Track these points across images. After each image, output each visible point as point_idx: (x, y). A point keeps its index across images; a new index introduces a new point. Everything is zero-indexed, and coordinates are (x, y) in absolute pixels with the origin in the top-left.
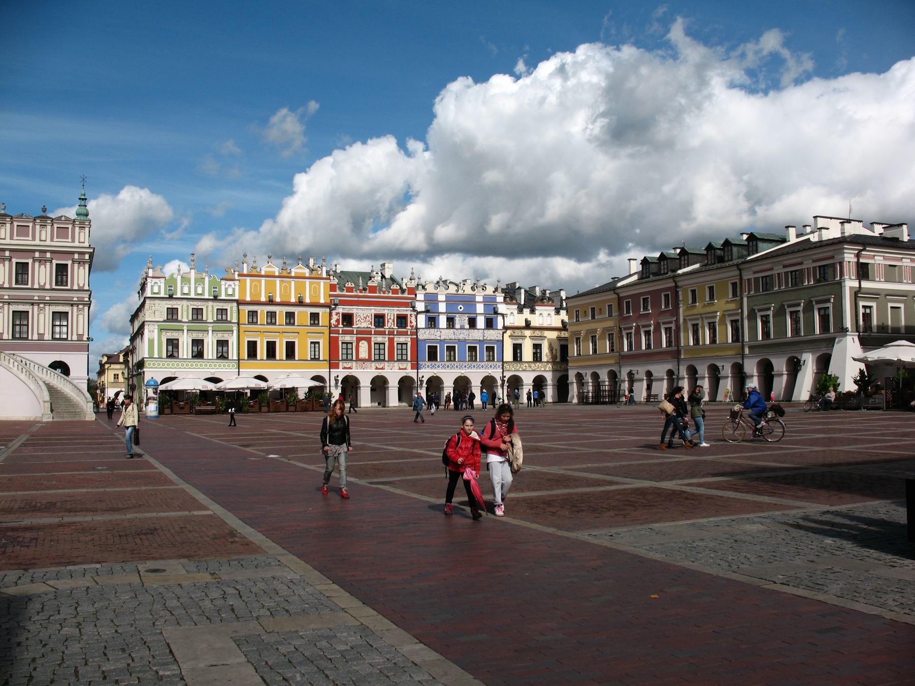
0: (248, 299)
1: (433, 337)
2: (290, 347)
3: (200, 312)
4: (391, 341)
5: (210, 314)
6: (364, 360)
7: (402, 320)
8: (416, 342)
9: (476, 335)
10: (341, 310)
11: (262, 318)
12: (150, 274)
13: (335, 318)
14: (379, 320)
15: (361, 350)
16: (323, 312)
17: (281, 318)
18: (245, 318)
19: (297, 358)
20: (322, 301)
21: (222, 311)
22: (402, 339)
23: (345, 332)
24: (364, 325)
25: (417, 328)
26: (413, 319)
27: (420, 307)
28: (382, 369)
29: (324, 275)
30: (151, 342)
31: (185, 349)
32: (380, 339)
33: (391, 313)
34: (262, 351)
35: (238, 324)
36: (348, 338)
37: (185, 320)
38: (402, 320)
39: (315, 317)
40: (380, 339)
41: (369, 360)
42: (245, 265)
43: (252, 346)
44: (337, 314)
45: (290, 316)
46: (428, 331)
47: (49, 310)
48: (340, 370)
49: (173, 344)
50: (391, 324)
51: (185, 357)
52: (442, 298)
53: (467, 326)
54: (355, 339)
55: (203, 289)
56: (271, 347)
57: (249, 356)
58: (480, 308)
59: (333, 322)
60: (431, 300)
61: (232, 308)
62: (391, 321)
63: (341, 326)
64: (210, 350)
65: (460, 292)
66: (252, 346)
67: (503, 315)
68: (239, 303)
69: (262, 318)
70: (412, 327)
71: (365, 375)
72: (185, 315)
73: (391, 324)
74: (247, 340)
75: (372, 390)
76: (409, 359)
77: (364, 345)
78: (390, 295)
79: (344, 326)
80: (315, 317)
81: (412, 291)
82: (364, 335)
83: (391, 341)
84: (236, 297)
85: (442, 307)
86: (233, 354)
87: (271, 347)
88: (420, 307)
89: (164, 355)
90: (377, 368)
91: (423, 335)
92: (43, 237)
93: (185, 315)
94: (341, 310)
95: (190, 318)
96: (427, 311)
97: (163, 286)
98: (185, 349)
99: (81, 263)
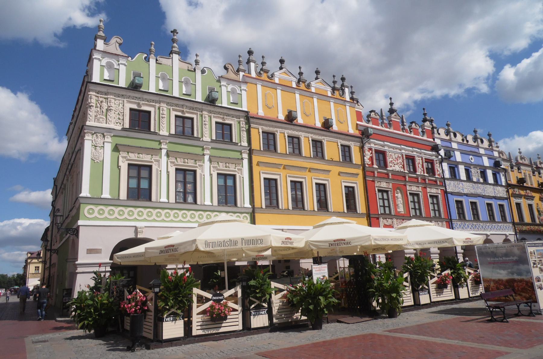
0: (261, 113)
1: (457, 191)
3: (144, 173)
5: (206, 128)
8: (445, 192)
9: (490, 191)
11: (282, 145)
13: (368, 155)
17: (307, 148)
22: (433, 191)
24: (397, 168)
25: (444, 179)
27: (442, 152)
30: (98, 165)
32: (414, 189)
33: (421, 156)
36: (384, 185)
37: (161, 133)
39: (346, 151)
42: (252, 65)
44: (370, 149)
45: (318, 145)
46: (452, 182)
49: (141, 173)
51: (164, 199)
53: (481, 180)
54: (391, 186)
58: (486, 162)
59: (367, 159)
63: (375, 166)
64: (207, 190)
67: (505, 170)
70: (439, 175)
74: (263, 176)
76: (443, 216)
78: (412, 135)
80: (346, 151)
85: (458, 157)
89: (123, 195)
91: (451, 186)
95: (173, 132)
97: (123, 69)
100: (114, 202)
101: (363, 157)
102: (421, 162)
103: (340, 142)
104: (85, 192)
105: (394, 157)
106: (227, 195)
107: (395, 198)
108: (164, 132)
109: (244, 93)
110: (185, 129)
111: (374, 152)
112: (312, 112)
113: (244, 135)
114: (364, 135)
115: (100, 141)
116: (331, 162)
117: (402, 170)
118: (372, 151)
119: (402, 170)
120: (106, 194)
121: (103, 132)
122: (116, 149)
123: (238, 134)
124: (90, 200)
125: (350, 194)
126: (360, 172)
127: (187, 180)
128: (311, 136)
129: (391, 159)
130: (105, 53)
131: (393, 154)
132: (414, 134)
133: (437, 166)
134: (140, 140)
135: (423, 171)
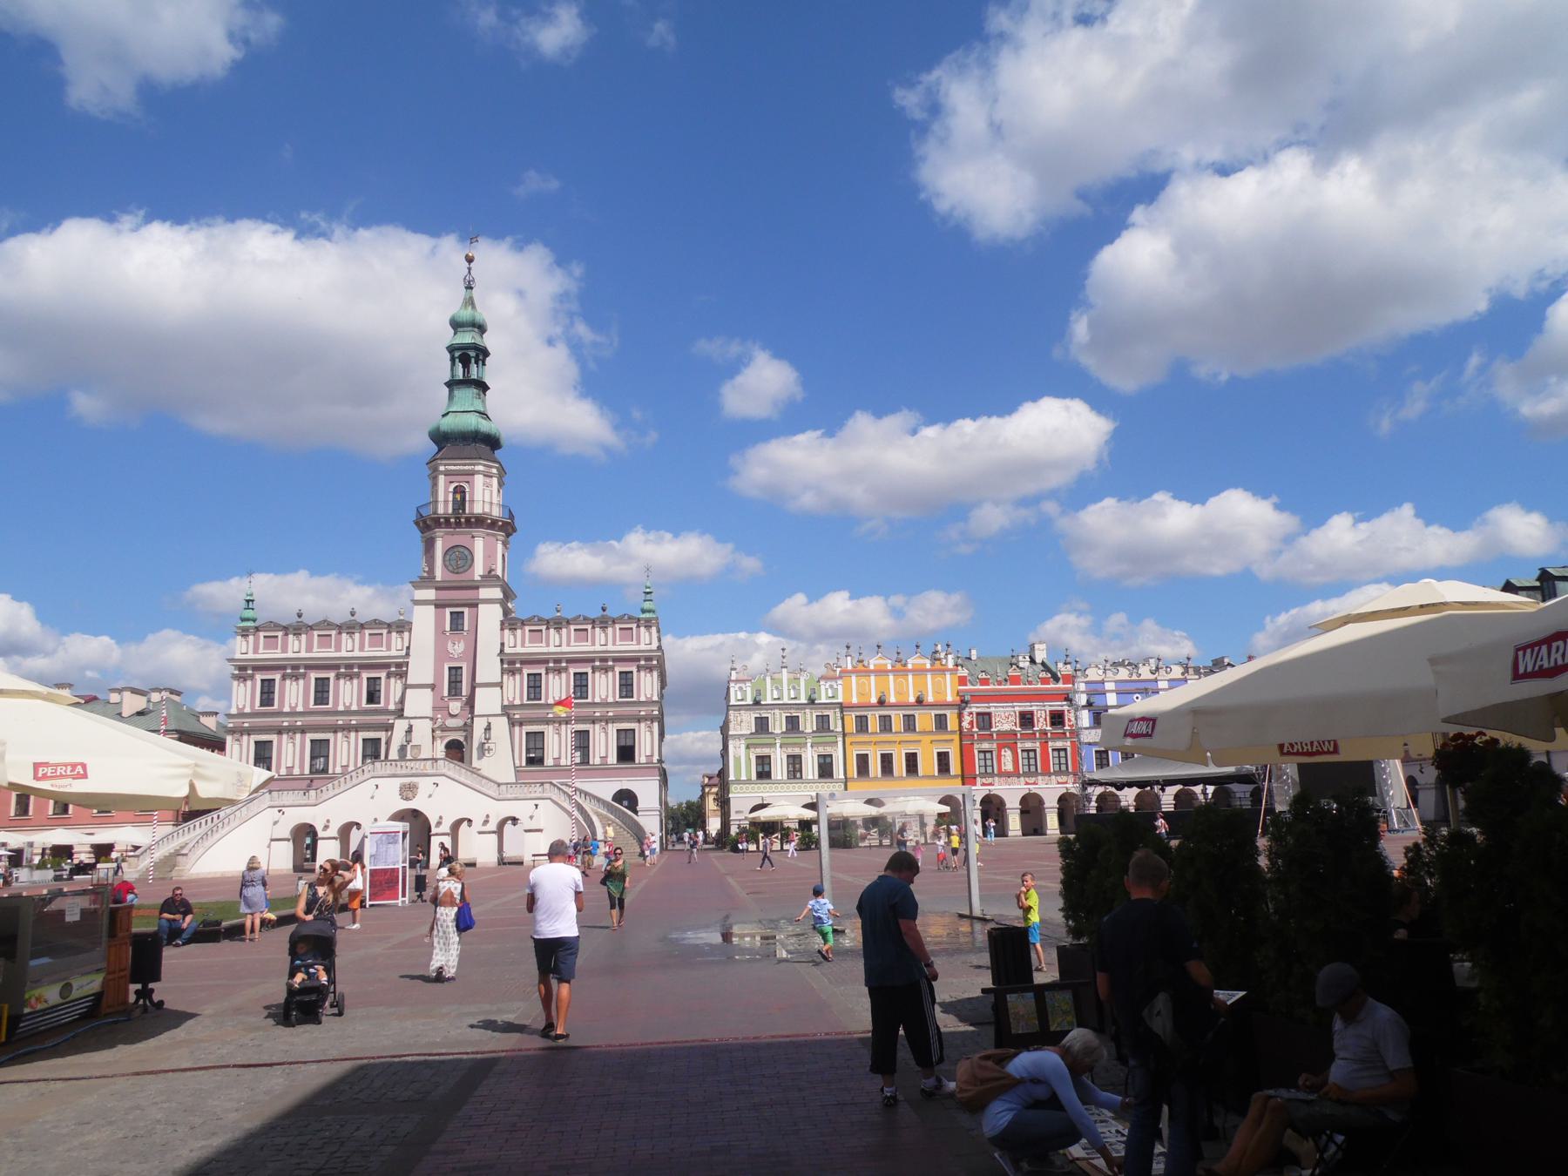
0: (855, 700)
2: (912, 761)
4: (1044, 745)
5: (808, 722)
7: (1057, 719)
10: (975, 708)
11: (873, 724)
12: (734, 676)
13: (967, 719)
14: (1027, 719)
16: (951, 716)
17: (897, 723)
18: (851, 725)
19: (920, 773)
20: (949, 699)
21: (823, 722)
23: (982, 738)
24: (1006, 727)
29: (951, 665)
30: (737, 760)
31: (779, 768)
34: (875, 766)
35: (844, 735)
36: (986, 746)
38: (1057, 719)
41: (1016, 773)
43: (863, 761)
47: (612, 729)
49: (764, 761)
50: (1042, 723)
52: (1109, 686)
55: (797, 691)
56: (887, 760)
57: (859, 773)
59: (965, 724)
60: (1096, 690)
61: (835, 716)
65: (1134, 677)
66: (863, 761)
68: (842, 707)
69: (873, 724)
71: (1011, 793)
72: (778, 725)
73: (1042, 723)
75: (1023, 812)
80: (941, 722)
81: (1069, 679)
82: (1008, 740)
83: (1044, 745)
84: (840, 700)
86: (838, 772)
87: (887, 760)
88: (1082, 699)
89: (754, 776)
92: (604, 641)
93: (778, 725)
94: (975, 708)
96: (1089, 704)
98: (779, 768)
99: (650, 669)
100: (749, 781)
101: (960, 722)
103: (934, 713)
104: (732, 777)
106: (825, 770)
107: (999, 756)
108: (778, 731)
109: (840, 688)
110: (793, 723)
112: (899, 690)
113: (839, 723)
114: (962, 704)
115: (737, 742)
116: (924, 733)
120: (744, 778)
121: (740, 737)
122: (748, 747)
123: (835, 725)
124: (738, 781)
125: (943, 758)
126: (956, 737)
127: (795, 763)
128: (901, 713)
130: (737, 681)
133: (1069, 716)
134: (764, 739)
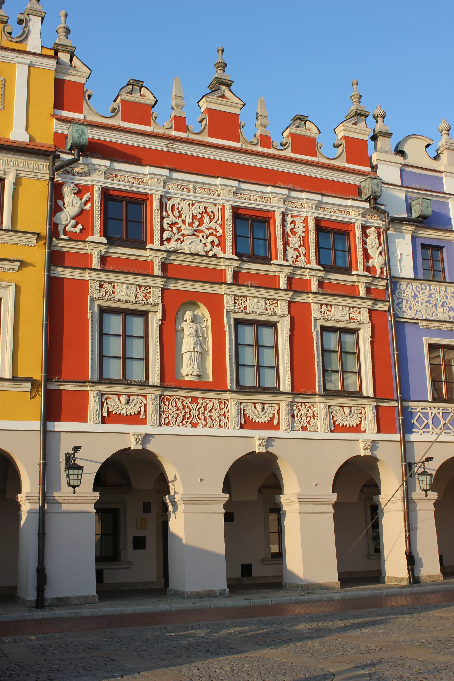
4: (299, 316)
6: (199, 385)
13: (71, 204)
15: (187, 343)
20: (18, 134)
26: (372, 240)
28: (270, 425)
32: (255, 305)
40: (255, 305)
41: (217, 387)
46: (424, 291)
48: (92, 424)
50: (296, 255)
62: (294, 241)
63: (97, 237)
73: (296, 255)
75: (228, 517)
77: (193, 333)
79: (112, 242)
90: (247, 423)
101: (55, 208)
102: (300, 229)
105: (186, 212)
111: (97, 196)
117: (217, 250)
118: (92, 195)
119: (217, 250)
129: (171, 219)
131: (185, 206)
132: (293, 152)
135: (307, 254)
